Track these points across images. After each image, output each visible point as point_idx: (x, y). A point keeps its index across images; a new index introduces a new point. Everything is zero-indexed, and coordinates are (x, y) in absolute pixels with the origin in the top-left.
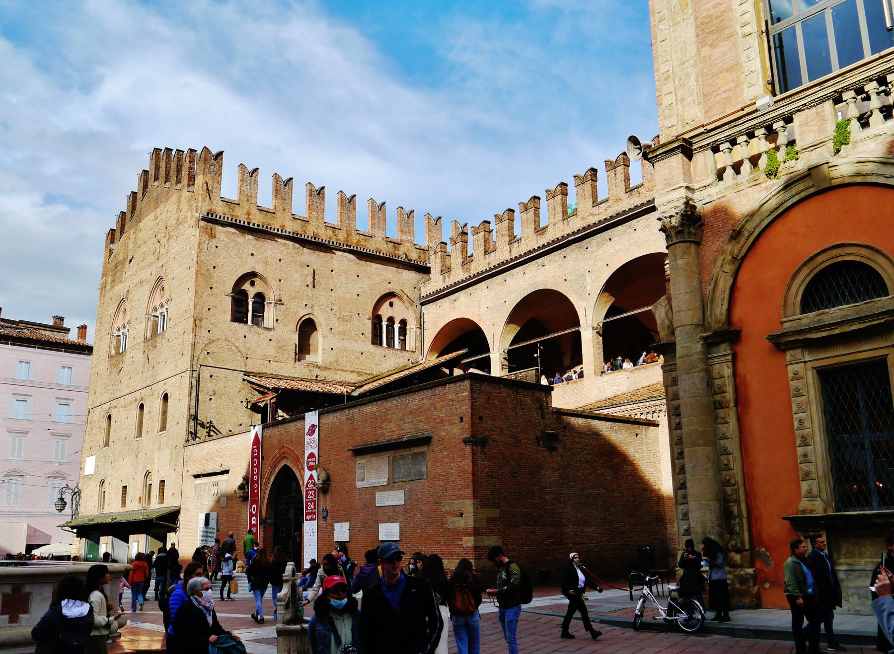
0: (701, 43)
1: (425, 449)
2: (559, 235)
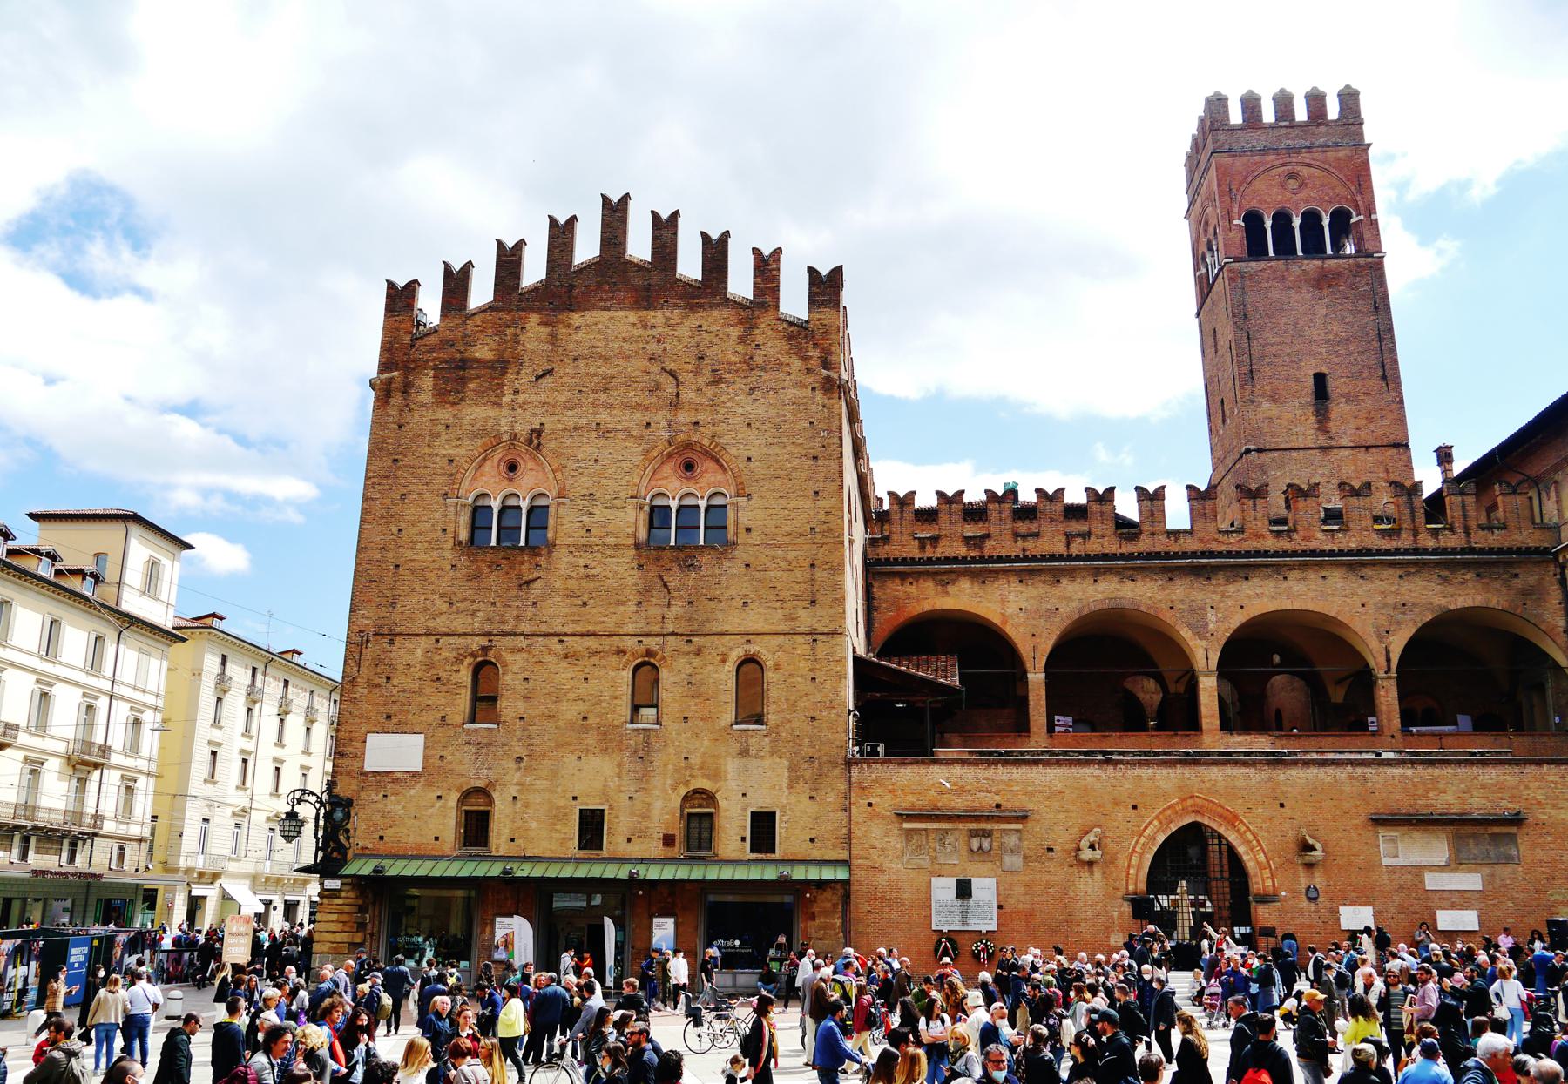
1: (1514, 830)
2: (1160, 548)
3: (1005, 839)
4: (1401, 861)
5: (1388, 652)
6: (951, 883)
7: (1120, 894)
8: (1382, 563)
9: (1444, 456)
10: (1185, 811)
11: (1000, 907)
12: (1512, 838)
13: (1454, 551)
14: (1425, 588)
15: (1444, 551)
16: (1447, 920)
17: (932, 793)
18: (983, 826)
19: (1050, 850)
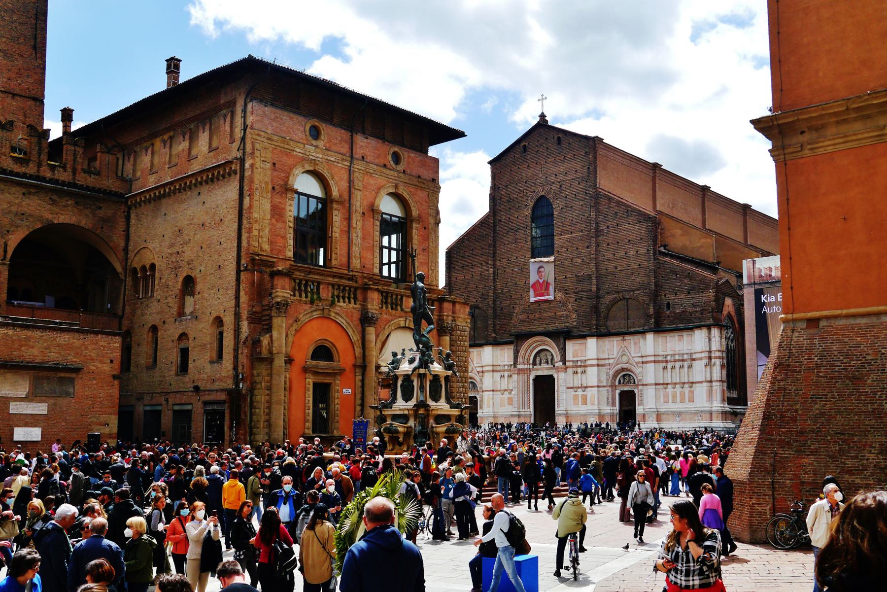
0: (272, 216)
1: (74, 375)
5: (6, 245)
8: (13, 182)
9: (67, 115)
12: (72, 381)
13: (63, 183)
14: (39, 205)
15: (56, 182)
16: (20, 434)
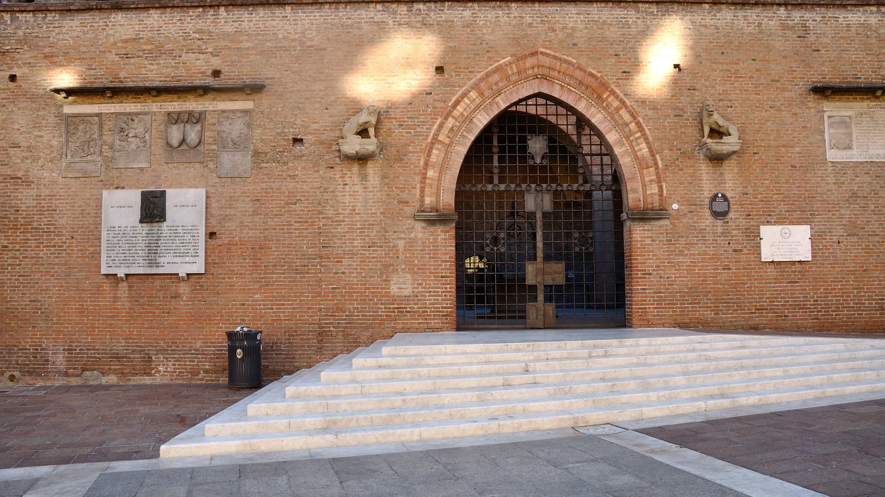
3: (226, 127)
4: (855, 155)
6: (133, 197)
7: (409, 210)
10: (523, 76)
11: (211, 235)
17: (112, 57)
18: (192, 105)
19: (297, 141)
